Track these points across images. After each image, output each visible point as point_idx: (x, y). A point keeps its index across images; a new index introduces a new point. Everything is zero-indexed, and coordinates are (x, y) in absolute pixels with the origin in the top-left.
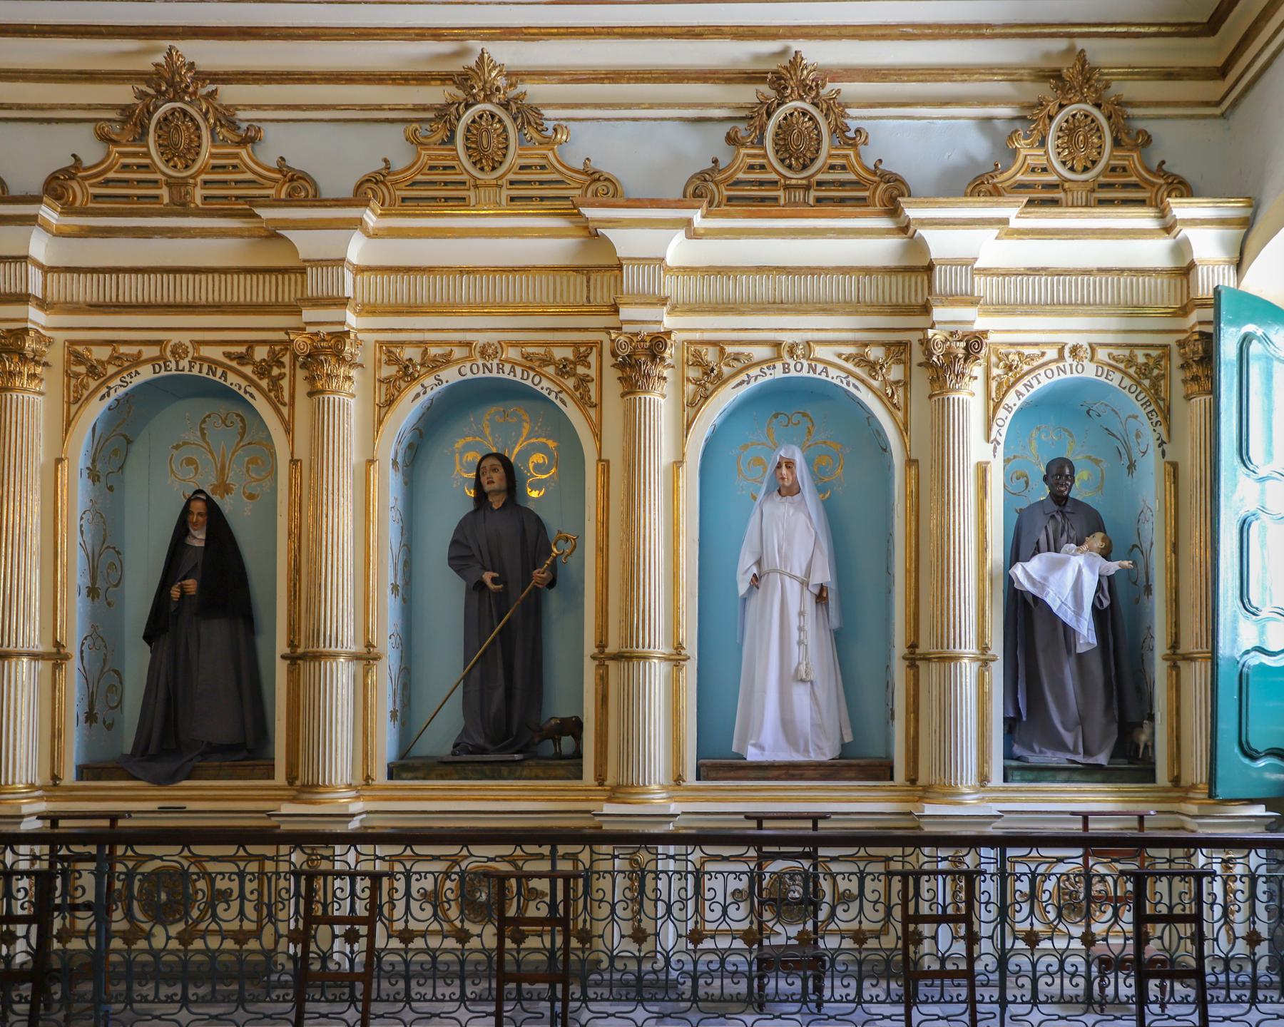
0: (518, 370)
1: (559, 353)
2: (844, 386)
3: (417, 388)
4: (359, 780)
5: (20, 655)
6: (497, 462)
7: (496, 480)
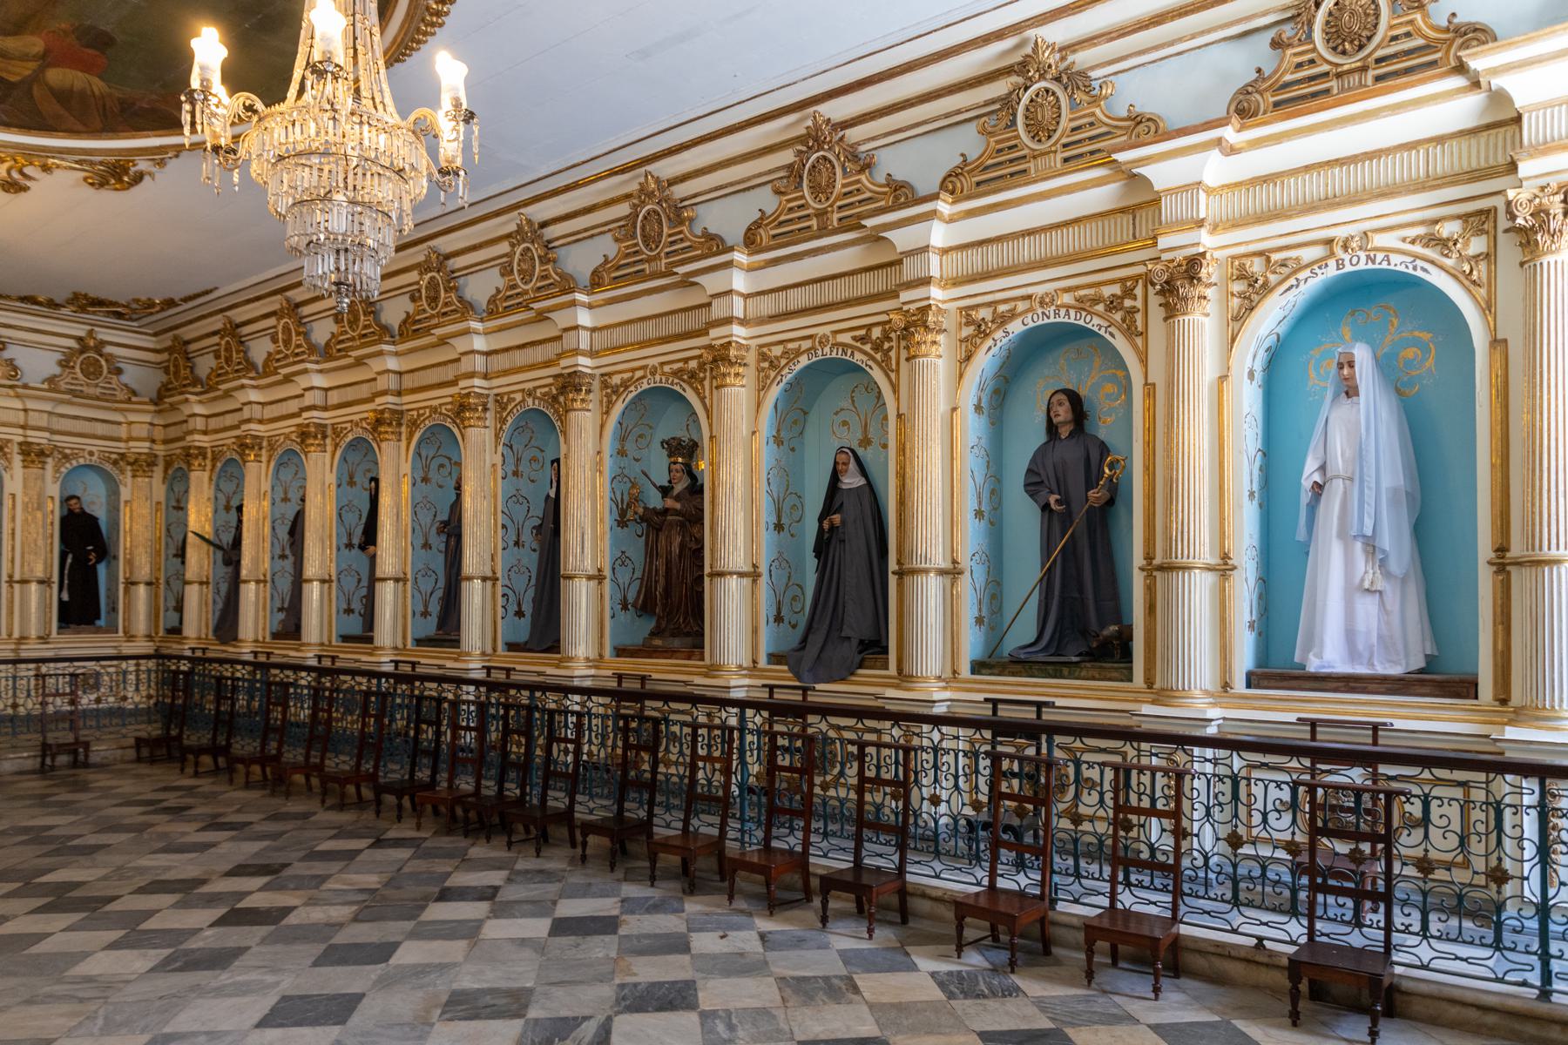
0: (1072, 312)
1: (1107, 291)
2: (1410, 271)
3: (990, 342)
4: (948, 674)
5: (731, 574)
6: (1063, 397)
7: (1063, 413)
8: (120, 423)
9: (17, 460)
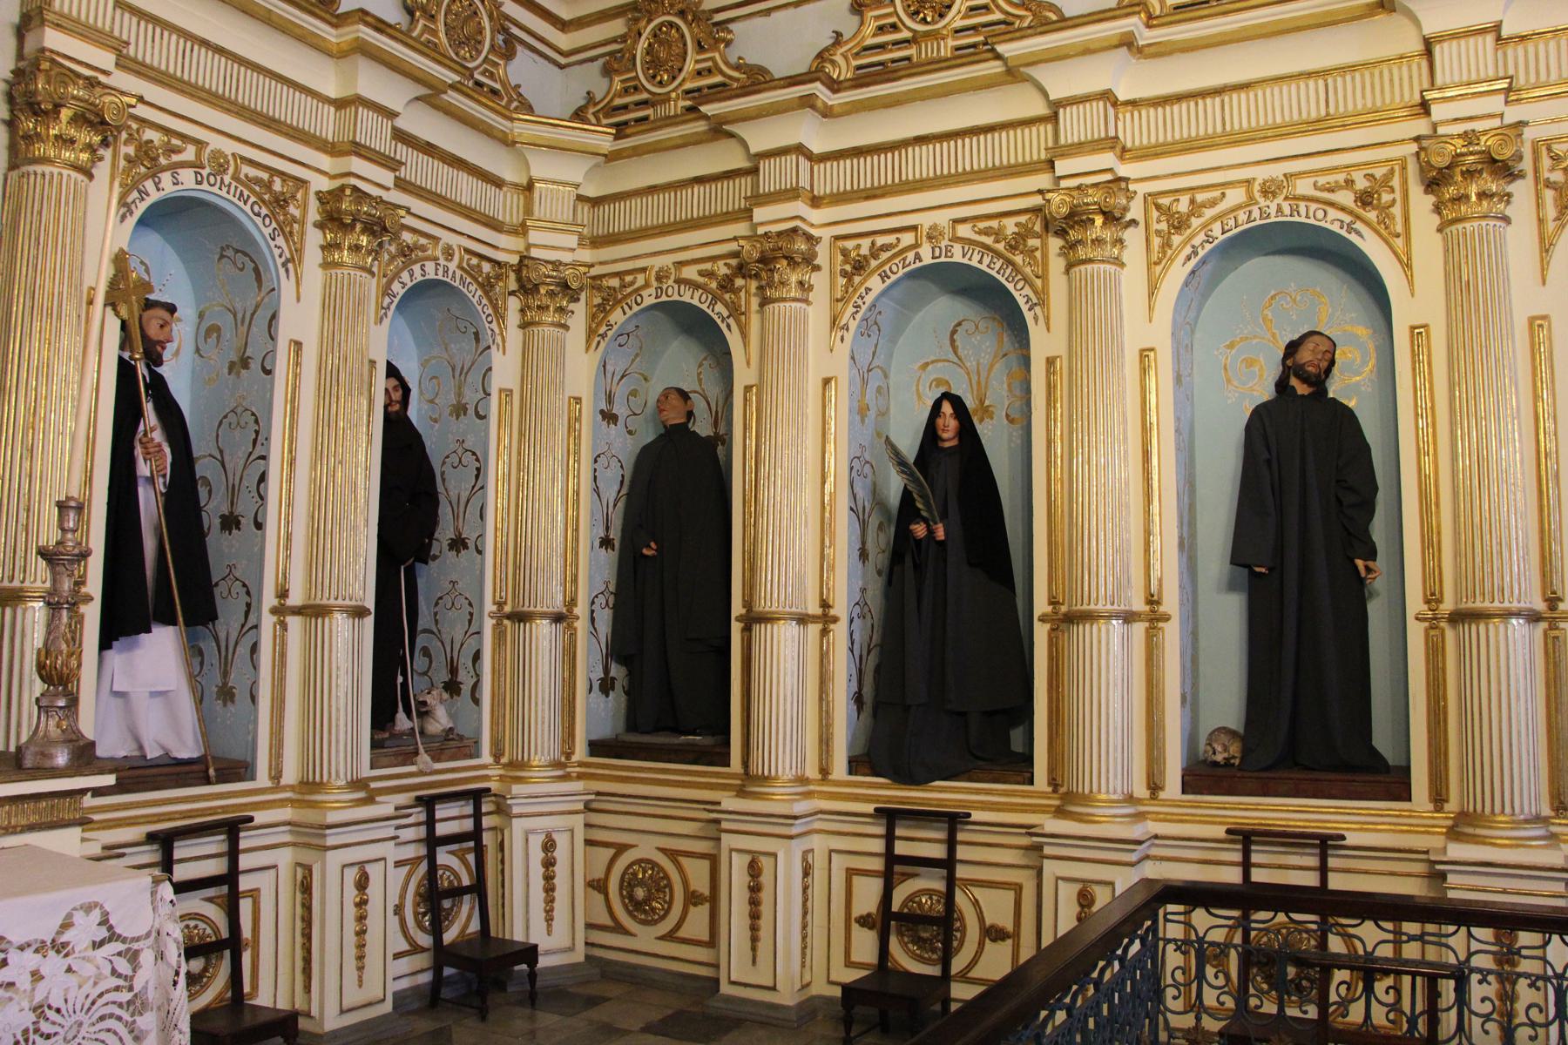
8: (498, 183)
9: (314, 239)
